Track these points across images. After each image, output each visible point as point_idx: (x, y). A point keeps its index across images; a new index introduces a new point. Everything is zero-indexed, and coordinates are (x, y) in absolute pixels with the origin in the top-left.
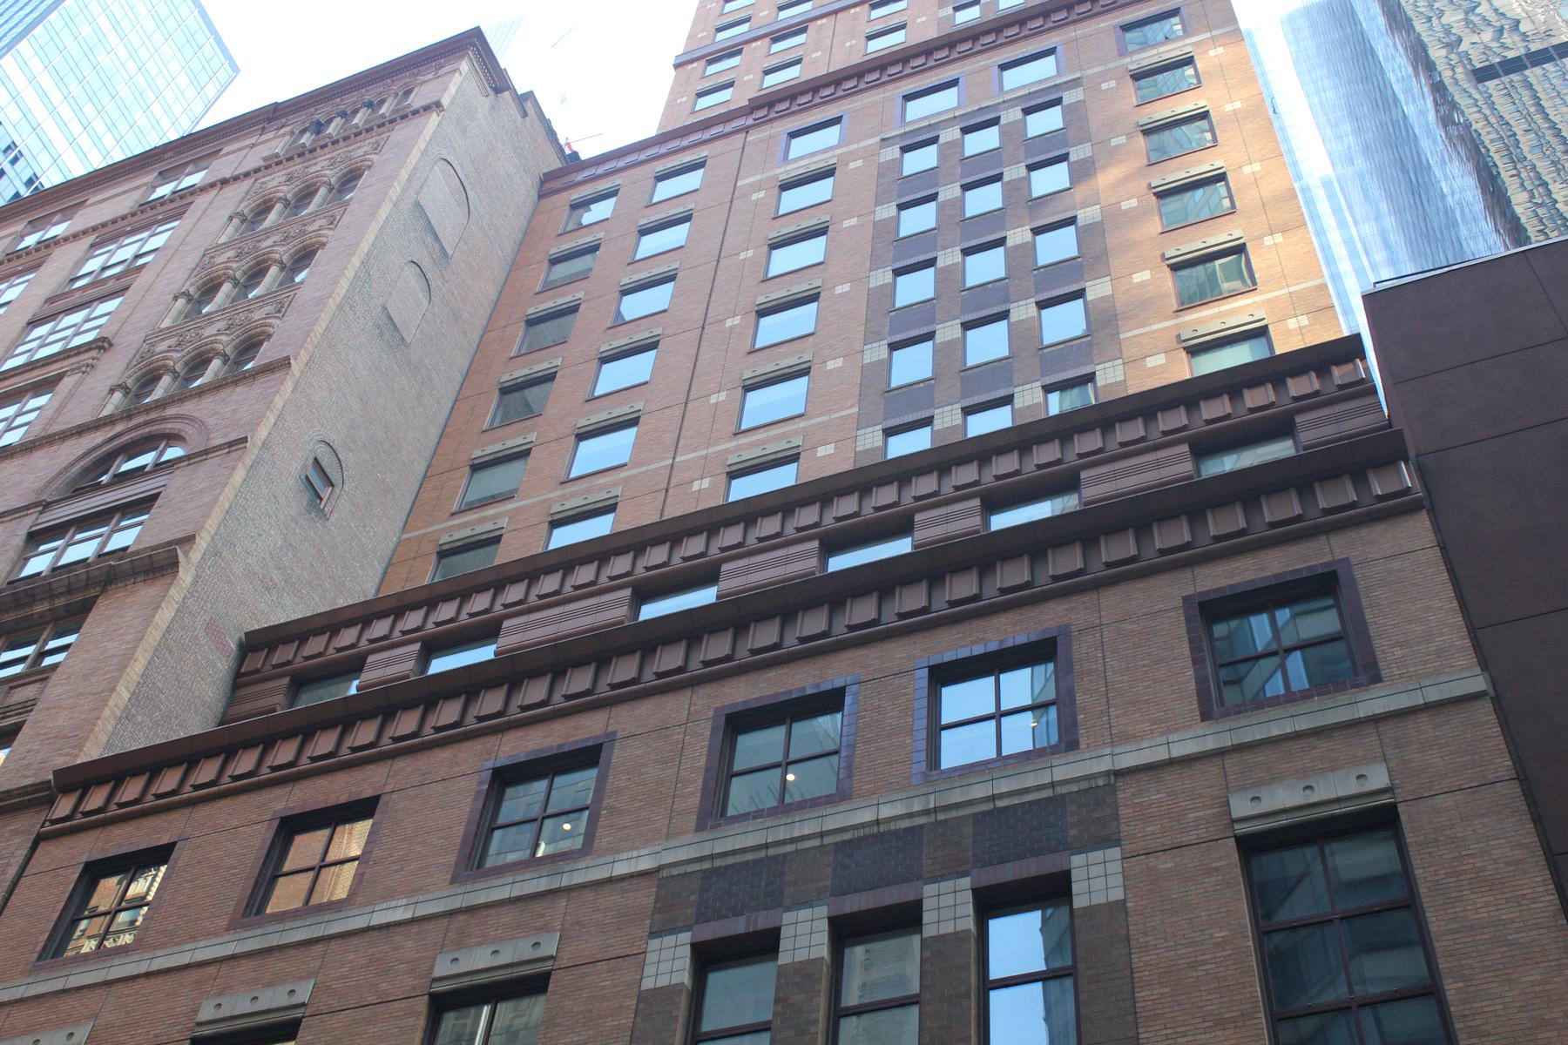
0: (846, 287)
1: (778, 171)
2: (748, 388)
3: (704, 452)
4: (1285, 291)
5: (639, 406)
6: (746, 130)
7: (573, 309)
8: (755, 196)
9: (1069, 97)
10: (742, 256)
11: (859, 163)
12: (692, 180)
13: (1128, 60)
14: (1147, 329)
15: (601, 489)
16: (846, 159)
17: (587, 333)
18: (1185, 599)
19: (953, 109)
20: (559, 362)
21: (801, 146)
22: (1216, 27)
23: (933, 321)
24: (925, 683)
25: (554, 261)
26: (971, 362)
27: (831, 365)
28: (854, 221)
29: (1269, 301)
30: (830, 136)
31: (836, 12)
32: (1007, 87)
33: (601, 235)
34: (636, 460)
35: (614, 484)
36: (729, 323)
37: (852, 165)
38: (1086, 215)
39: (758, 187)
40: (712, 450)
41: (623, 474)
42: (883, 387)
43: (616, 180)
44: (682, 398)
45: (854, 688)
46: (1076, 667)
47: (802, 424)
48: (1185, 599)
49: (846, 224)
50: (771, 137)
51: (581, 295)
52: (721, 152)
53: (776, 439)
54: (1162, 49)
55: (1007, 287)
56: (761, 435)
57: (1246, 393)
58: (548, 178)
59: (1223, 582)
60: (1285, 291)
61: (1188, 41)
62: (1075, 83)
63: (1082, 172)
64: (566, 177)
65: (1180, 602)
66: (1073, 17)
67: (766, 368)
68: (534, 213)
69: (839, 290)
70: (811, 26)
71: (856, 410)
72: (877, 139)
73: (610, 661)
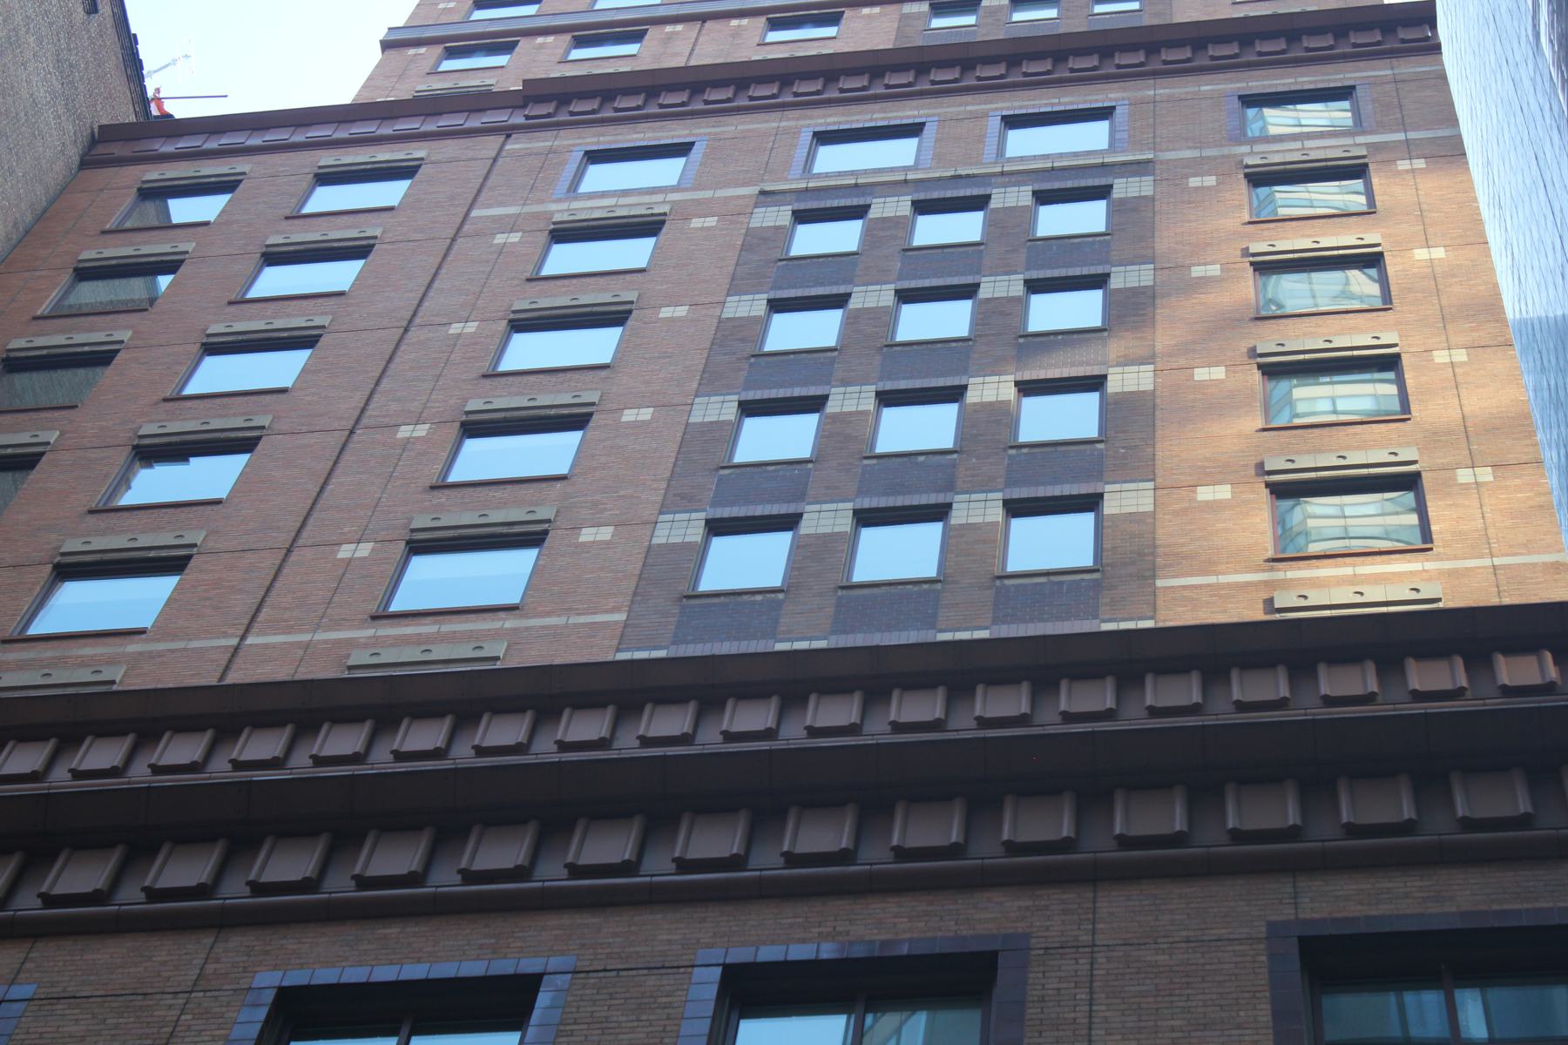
0: (646, 414)
1: (553, 207)
2: (420, 546)
3: (306, 637)
4: (1487, 562)
5: (196, 537)
6: (508, 131)
7: (101, 358)
8: (500, 239)
9: (1124, 188)
10: (455, 329)
11: (711, 221)
12: (390, 193)
13: (1245, 149)
14: (1212, 579)
15: (83, 665)
16: (685, 212)
17: (117, 404)
18: (1271, 926)
19: (906, 169)
20: (53, 436)
21: (601, 177)
22: (1418, 128)
23: (801, 496)
24: (711, 992)
25: (85, 273)
26: (859, 576)
27: (587, 535)
28: (681, 311)
29: (1452, 573)
30: (666, 172)
31: (703, 18)
32: (1009, 153)
33: (189, 247)
34: (167, 624)
35: (112, 661)
36: (404, 432)
37: (696, 223)
38: (1120, 381)
39: (510, 225)
40: (321, 636)
41: (133, 647)
42: (684, 588)
43: (241, 165)
44: (284, 539)
45: (562, 981)
46: (1031, 1012)
47: (510, 623)
48: (1271, 926)
49: (666, 312)
50: (551, 151)
51: (125, 335)
52: (452, 161)
53: (452, 638)
54: (1309, 144)
55: (954, 465)
56: (427, 628)
57: (1412, 666)
58: (108, 134)
59: (1355, 910)
60: (1487, 562)
61: (1361, 139)
62: (1139, 168)
63: (1129, 311)
64: (138, 142)
65: (1262, 930)
66: (1155, 65)
67: (462, 516)
68: (65, 189)
69: (629, 416)
70: (653, 33)
71: (622, 617)
72: (754, 190)
73: (54, 856)
